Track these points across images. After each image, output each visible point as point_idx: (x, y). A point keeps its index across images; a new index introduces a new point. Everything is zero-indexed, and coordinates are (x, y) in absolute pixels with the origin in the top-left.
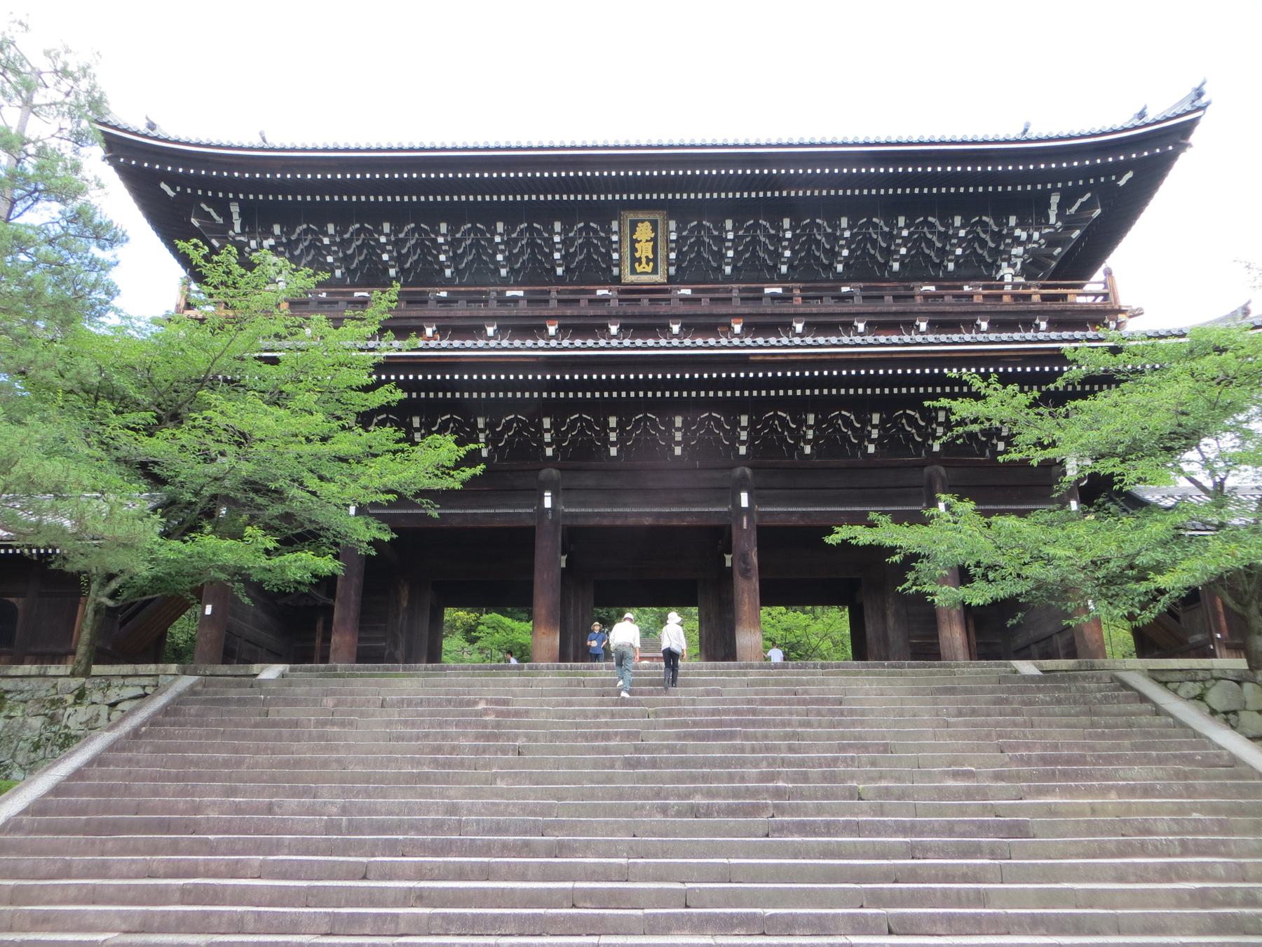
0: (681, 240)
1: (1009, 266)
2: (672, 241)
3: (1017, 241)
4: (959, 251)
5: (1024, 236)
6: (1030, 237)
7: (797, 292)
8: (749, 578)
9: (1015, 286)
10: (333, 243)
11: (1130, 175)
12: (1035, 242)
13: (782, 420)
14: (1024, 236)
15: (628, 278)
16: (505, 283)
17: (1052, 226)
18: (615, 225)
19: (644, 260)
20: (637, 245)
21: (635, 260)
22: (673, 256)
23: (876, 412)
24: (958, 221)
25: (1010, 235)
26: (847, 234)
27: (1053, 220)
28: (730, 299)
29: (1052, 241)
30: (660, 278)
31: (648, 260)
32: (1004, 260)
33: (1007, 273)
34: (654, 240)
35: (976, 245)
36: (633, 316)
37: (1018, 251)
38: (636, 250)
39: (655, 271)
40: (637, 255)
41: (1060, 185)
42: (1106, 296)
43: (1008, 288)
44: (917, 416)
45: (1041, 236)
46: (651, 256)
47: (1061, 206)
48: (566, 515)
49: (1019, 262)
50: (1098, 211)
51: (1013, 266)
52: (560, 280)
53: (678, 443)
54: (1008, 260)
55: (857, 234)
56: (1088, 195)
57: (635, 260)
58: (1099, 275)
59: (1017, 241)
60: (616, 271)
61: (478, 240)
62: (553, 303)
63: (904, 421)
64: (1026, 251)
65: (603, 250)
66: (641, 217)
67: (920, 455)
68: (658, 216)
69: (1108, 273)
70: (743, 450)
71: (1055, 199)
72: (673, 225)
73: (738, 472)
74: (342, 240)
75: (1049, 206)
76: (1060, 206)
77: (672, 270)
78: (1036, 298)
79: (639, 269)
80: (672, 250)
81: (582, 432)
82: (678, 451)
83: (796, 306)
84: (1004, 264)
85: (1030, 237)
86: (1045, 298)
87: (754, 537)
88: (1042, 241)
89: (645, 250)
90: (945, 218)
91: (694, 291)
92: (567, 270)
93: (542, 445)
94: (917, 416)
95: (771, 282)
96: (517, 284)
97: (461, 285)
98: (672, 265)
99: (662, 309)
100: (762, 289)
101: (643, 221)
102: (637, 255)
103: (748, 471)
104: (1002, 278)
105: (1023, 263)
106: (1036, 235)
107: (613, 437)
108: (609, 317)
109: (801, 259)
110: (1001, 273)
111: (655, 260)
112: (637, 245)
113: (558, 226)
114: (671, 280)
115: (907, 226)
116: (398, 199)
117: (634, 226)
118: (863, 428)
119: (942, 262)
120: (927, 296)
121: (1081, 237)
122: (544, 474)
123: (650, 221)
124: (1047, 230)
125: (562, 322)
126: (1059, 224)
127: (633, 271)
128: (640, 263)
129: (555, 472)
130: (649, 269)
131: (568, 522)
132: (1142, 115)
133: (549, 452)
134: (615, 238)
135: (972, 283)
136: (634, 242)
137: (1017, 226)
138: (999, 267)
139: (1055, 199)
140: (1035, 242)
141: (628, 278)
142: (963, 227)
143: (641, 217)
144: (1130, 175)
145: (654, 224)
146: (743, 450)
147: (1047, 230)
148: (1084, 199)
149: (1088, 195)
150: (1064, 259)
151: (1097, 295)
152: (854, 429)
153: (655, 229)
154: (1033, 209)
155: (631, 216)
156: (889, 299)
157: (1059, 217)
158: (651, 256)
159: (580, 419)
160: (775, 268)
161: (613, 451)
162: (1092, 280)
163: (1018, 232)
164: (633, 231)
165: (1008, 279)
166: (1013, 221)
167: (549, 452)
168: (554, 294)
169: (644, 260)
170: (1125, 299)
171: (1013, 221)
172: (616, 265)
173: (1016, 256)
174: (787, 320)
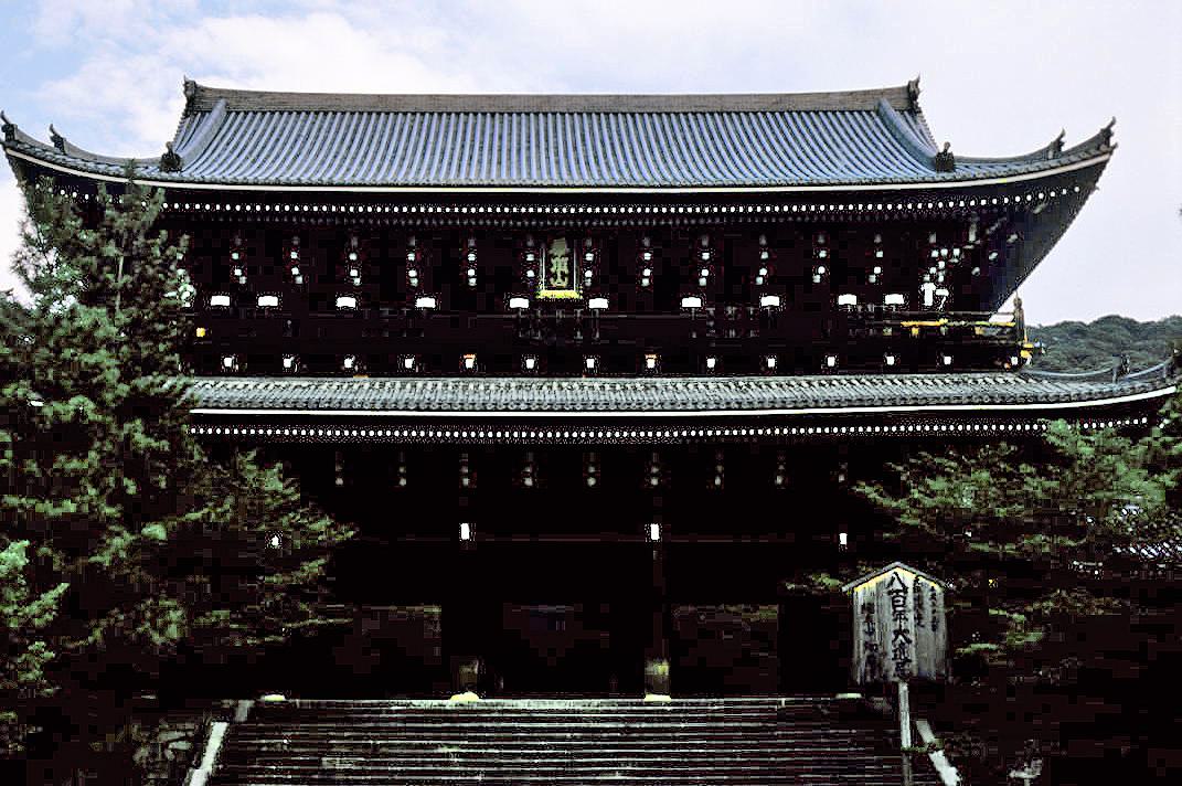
15: (544, 293)
19: (559, 275)
21: (550, 275)
27: (972, 238)
34: (568, 255)
38: (552, 265)
39: (570, 287)
40: (553, 270)
46: (566, 271)
57: (550, 275)
58: (1008, 306)
69: (1018, 304)
89: (560, 265)
102: (553, 270)
106: (956, 252)
111: (570, 276)
112: (553, 261)
127: (550, 287)
128: (556, 278)
130: (564, 284)
132: (1058, 144)
136: (549, 258)
154: (951, 231)
158: (566, 271)
162: (1000, 310)
169: (559, 275)
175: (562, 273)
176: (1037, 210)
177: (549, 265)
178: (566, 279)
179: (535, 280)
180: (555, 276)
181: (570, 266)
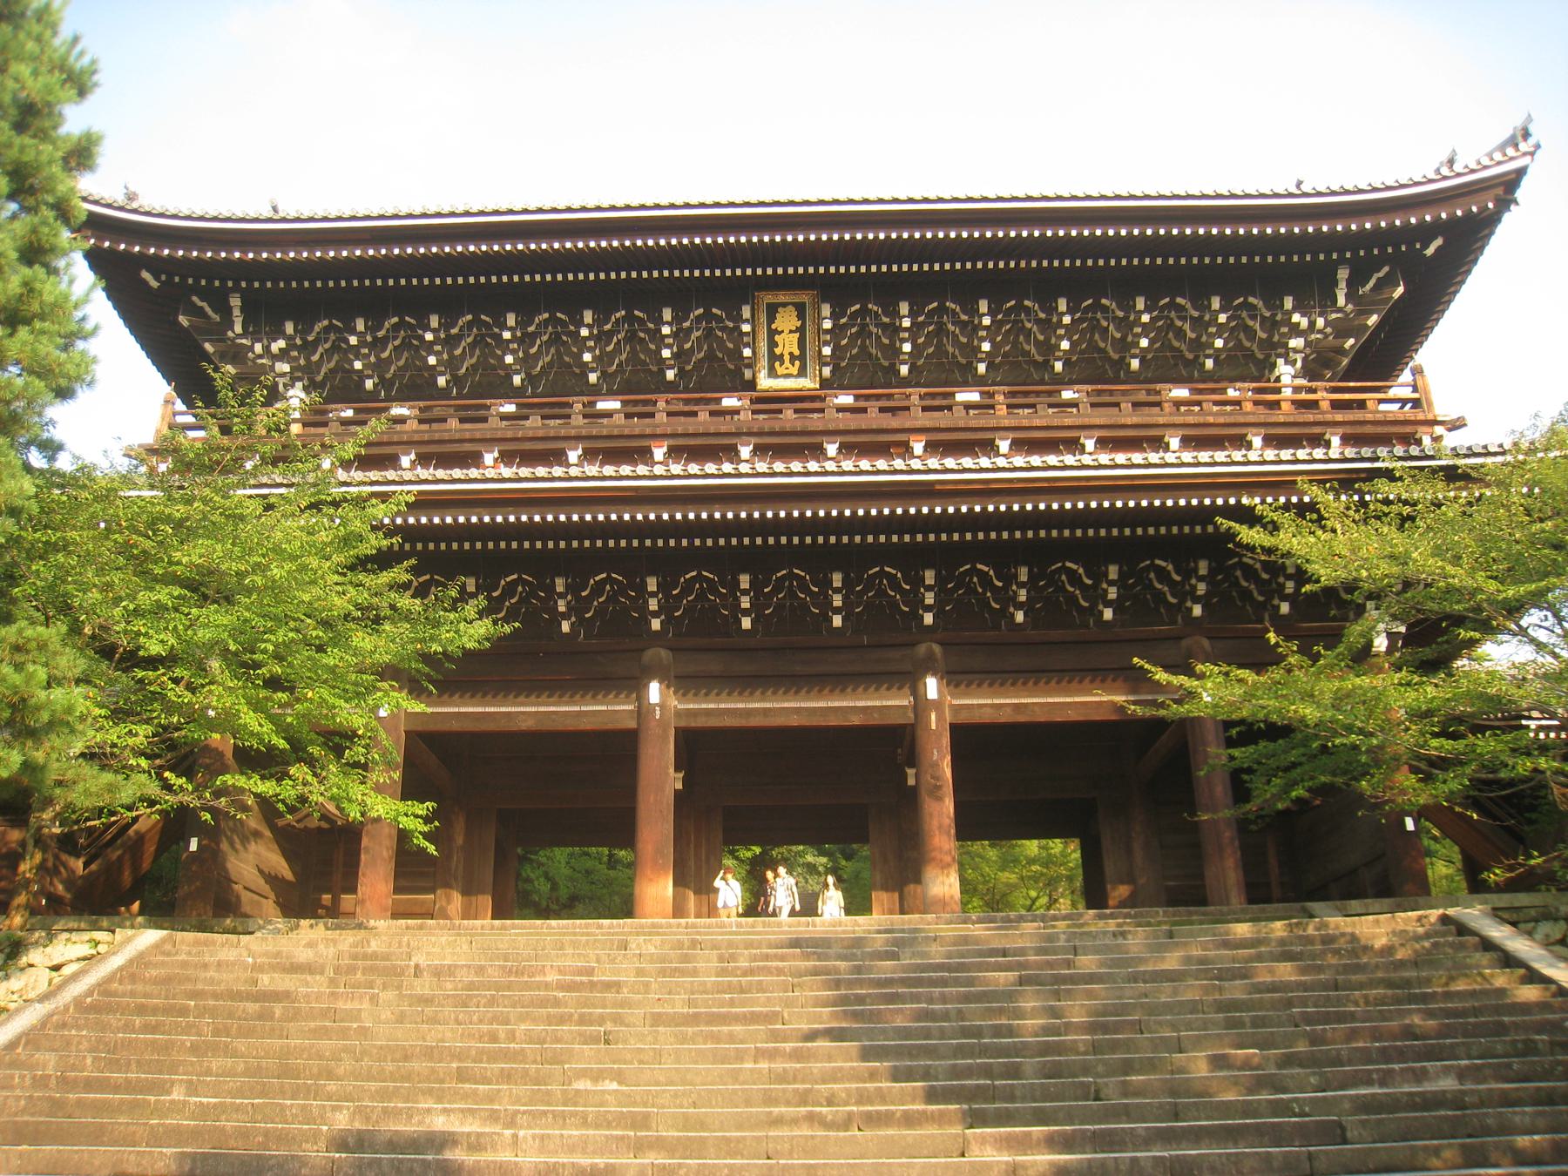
0: (837, 331)
1: (1286, 363)
2: (827, 331)
3: (1295, 330)
4: (1219, 343)
5: (1304, 323)
6: (1312, 324)
7: (1000, 398)
8: (940, 799)
9: (1297, 389)
10: (362, 343)
11: (1439, 242)
12: (1319, 332)
13: (981, 574)
14: (1304, 323)
15: (765, 382)
16: (596, 392)
17: (1340, 310)
18: (746, 312)
19: (787, 358)
20: (777, 338)
22: (827, 351)
23: (1113, 563)
24: (1216, 303)
25: (1288, 322)
26: (1067, 320)
27: (1341, 301)
28: (908, 408)
29: (1342, 330)
30: (808, 383)
31: (793, 357)
32: (1279, 356)
33: (1285, 372)
35: (1242, 336)
36: (772, 433)
37: (1296, 343)
39: (802, 373)
40: (778, 351)
41: (1348, 255)
42: (1416, 403)
43: (1287, 393)
44: (1170, 567)
45: (1327, 324)
46: (797, 353)
47: (1353, 284)
48: (678, 713)
49: (1299, 357)
50: (1400, 290)
51: (1294, 363)
52: (671, 387)
53: (837, 611)
54: (1286, 356)
55: (1081, 320)
56: (1386, 269)
57: (774, 358)
58: (1406, 376)
59: (1295, 330)
60: (748, 374)
61: (558, 335)
62: (661, 417)
63: (1152, 575)
64: (1308, 344)
65: (731, 346)
66: (782, 298)
67: (1174, 622)
68: (805, 297)
69: (1418, 371)
70: (928, 619)
71: (1343, 274)
72: (826, 310)
73: (922, 649)
74: (375, 339)
75: (1336, 284)
76: (1349, 283)
77: (827, 371)
78: (1325, 405)
79: (780, 370)
80: (826, 343)
81: (701, 596)
82: (837, 621)
83: (1000, 417)
84: (1280, 361)
85: (1312, 324)
86: (1336, 405)
87: (946, 740)
88: (1329, 330)
89: (788, 344)
90: (1200, 301)
91: (857, 398)
92: (681, 373)
93: (646, 616)
94: (1170, 567)
95: (964, 384)
96: (611, 393)
97: (534, 395)
98: (827, 364)
99: (815, 421)
100: (953, 394)
101: (784, 305)
102: (778, 351)
103: (937, 649)
104: (1278, 379)
105: (1304, 360)
106: (1320, 322)
107: (745, 603)
108: (738, 434)
109: (1005, 355)
110: (1277, 373)
111: (802, 358)
112: (777, 338)
113: (667, 314)
114: (825, 384)
115: (1148, 310)
116: (449, 281)
117: (772, 311)
118: (1096, 586)
119: (1197, 357)
120: (1178, 403)
121: (1380, 325)
122: (649, 654)
123: (794, 304)
124: (1334, 316)
125: (673, 442)
126: (1350, 306)
127: (772, 373)
129: (664, 654)
130: (794, 371)
131: (683, 724)
133: (656, 624)
134: (746, 328)
135: (1238, 385)
136: (772, 333)
137: (1295, 309)
138: (1274, 365)
139: (1343, 274)
140: (1319, 332)
141: (765, 382)
142: (1223, 310)
143: (782, 298)
144: (1439, 242)
145: (800, 309)
146: (928, 619)
147: (1334, 316)
148: (1381, 274)
149: (1386, 269)
150: (1361, 353)
151: (1404, 402)
152: (1083, 587)
153: (801, 316)
154: (1315, 290)
155: (769, 298)
156: (1126, 406)
157: (1348, 297)
158: (797, 353)
159: (699, 577)
160: (970, 367)
161: (746, 623)
163: (1296, 318)
164: (771, 318)
165: (1286, 380)
166: (1288, 303)
167: (656, 624)
168: (661, 405)
169: (787, 358)
170: (1442, 407)
171: (1288, 303)
172: (749, 366)
173: (1295, 351)
174: (988, 435)
175: (791, 354)
176: (1430, 251)
177: (772, 344)
178: (797, 363)
179: (751, 363)
180: (781, 358)
181: (802, 344)
